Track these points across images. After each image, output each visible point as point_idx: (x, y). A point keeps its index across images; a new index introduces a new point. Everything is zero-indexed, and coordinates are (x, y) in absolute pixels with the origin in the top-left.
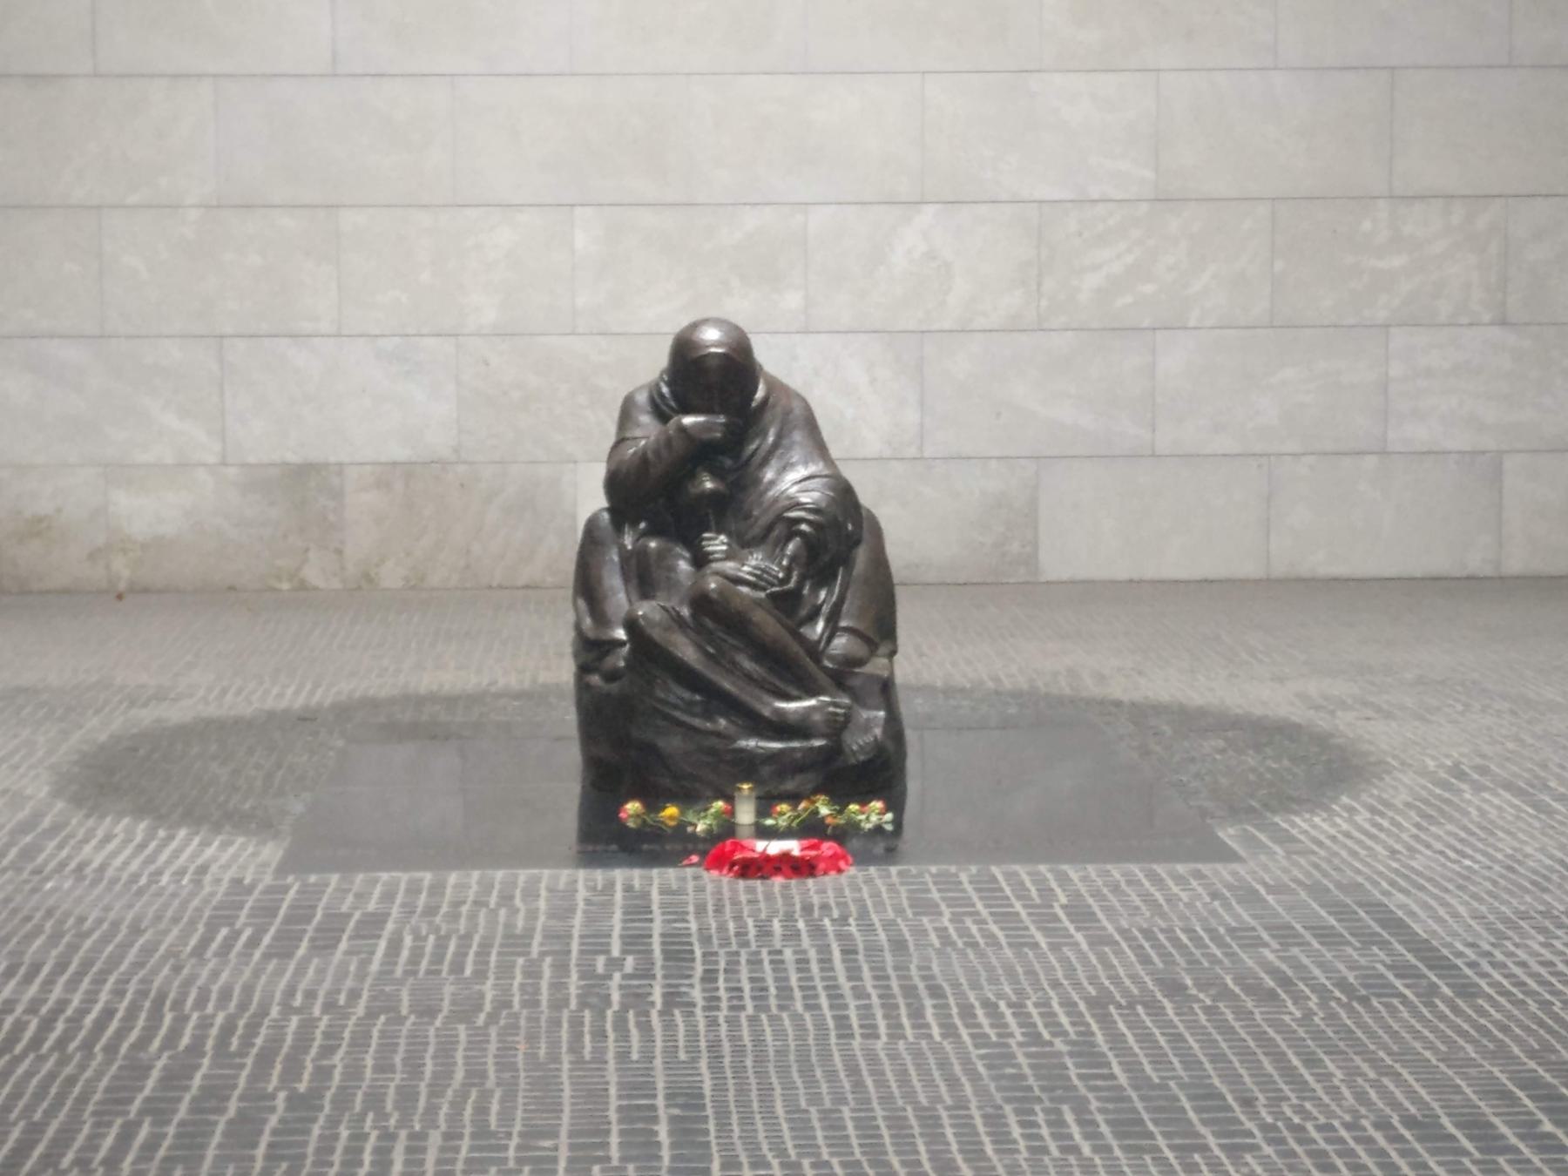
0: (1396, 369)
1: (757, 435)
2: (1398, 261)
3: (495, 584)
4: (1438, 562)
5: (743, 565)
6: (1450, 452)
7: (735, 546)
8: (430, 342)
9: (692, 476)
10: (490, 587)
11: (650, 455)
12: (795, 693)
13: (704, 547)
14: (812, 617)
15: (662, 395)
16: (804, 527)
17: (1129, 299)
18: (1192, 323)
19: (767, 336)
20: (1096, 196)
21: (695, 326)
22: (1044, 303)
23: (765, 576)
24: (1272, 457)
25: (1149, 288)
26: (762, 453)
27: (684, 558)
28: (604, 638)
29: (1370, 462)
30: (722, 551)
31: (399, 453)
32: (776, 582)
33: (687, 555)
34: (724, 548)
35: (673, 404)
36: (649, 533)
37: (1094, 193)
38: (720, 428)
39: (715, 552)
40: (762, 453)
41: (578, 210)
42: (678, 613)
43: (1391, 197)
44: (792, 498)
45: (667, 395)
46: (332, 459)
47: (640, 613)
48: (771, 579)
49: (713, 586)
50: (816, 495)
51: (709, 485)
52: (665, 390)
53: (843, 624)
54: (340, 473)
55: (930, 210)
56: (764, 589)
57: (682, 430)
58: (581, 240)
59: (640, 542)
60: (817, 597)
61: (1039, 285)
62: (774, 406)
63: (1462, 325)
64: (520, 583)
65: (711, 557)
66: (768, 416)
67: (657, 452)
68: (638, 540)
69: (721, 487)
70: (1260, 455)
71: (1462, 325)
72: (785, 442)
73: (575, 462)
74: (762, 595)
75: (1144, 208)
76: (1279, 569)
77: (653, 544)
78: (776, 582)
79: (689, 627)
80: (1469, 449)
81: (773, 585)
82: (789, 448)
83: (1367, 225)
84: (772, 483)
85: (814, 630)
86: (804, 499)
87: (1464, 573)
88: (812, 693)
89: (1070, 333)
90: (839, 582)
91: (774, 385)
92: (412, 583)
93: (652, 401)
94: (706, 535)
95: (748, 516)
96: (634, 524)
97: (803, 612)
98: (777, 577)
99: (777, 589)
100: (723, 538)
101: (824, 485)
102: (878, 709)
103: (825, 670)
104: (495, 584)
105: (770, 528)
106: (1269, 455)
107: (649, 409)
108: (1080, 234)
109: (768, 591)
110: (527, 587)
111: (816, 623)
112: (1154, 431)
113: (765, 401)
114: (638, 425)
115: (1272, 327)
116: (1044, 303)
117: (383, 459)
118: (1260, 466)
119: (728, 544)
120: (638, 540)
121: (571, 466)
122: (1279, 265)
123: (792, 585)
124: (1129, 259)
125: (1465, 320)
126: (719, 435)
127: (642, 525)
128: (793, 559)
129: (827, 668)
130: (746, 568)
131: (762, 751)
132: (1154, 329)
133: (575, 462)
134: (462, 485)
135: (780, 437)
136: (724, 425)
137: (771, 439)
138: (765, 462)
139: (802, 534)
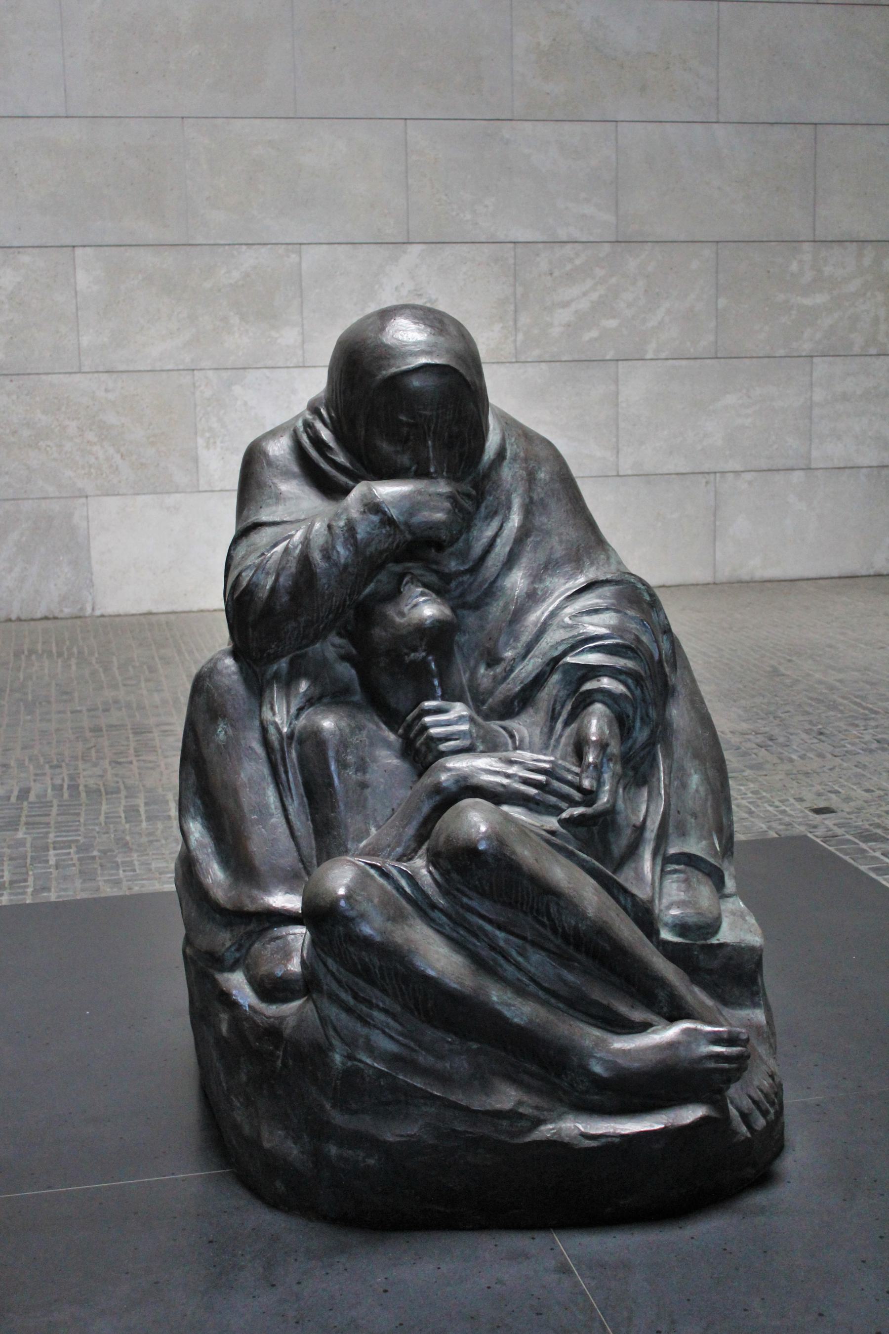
0: (819, 395)
1: (492, 514)
2: (820, 299)
3: (14, 617)
4: (851, 564)
5: (511, 762)
6: (862, 467)
7: (479, 720)
9: (394, 594)
10: (10, 620)
11: (317, 556)
12: (638, 1015)
13: (425, 728)
14: (633, 850)
15: (317, 441)
16: (606, 682)
17: (594, 333)
18: (648, 356)
19: (266, 371)
20: (565, 239)
21: (386, 315)
22: (520, 337)
23: (556, 784)
24: (718, 475)
25: (612, 323)
26: (502, 549)
27: (388, 745)
28: (251, 907)
29: (797, 477)
32: (577, 796)
33: (392, 737)
34: (465, 727)
35: (341, 458)
36: (311, 702)
37: (563, 235)
38: (447, 505)
39: (447, 738)
40: (502, 549)
41: (79, 251)
42: (411, 878)
43: (814, 241)
44: (567, 627)
45: (332, 444)
47: (342, 891)
48: (566, 789)
49: (483, 829)
50: (610, 618)
52: (326, 434)
53: (672, 851)
55: (416, 249)
56: (555, 811)
57: (373, 507)
58: (83, 279)
59: (302, 722)
60: (635, 811)
61: (515, 321)
63: (871, 355)
64: (39, 615)
65: (443, 747)
66: (508, 473)
67: (327, 553)
68: (297, 716)
69: (447, 612)
70: (708, 473)
71: (871, 355)
72: (540, 520)
73: (87, 497)
74: (552, 823)
75: (607, 248)
76: (725, 573)
77: (328, 724)
78: (577, 796)
79: (434, 906)
80: (875, 464)
81: (574, 803)
82: (548, 533)
83: (794, 267)
84: (533, 597)
85: (640, 877)
86: (594, 626)
87: (872, 572)
88: (672, 1019)
89: (543, 365)
90: (662, 768)
91: (509, 424)
93: (299, 450)
94: (429, 704)
95: (493, 660)
96: (288, 683)
97: (620, 845)
98: (579, 788)
99: (578, 811)
100: (459, 709)
101: (619, 596)
102: (755, 1005)
103: (665, 948)
104: (14, 617)
105: (538, 681)
106: (715, 473)
107: (295, 469)
108: (551, 274)
109: (564, 815)
110: (46, 618)
111: (641, 858)
112: (618, 452)
113: (501, 455)
114: (278, 497)
115: (717, 358)
116: (520, 337)
118: (707, 483)
119: (472, 720)
120: (300, 710)
121: (83, 500)
122: (722, 302)
123: (604, 799)
124: (594, 296)
125: (873, 351)
126: (440, 516)
127: (304, 686)
128: (603, 746)
129: (666, 943)
130: (513, 770)
132: (617, 360)
133: (87, 497)
135: (528, 511)
136: (451, 497)
137: (515, 520)
138: (510, 562)
139: (607, 696)
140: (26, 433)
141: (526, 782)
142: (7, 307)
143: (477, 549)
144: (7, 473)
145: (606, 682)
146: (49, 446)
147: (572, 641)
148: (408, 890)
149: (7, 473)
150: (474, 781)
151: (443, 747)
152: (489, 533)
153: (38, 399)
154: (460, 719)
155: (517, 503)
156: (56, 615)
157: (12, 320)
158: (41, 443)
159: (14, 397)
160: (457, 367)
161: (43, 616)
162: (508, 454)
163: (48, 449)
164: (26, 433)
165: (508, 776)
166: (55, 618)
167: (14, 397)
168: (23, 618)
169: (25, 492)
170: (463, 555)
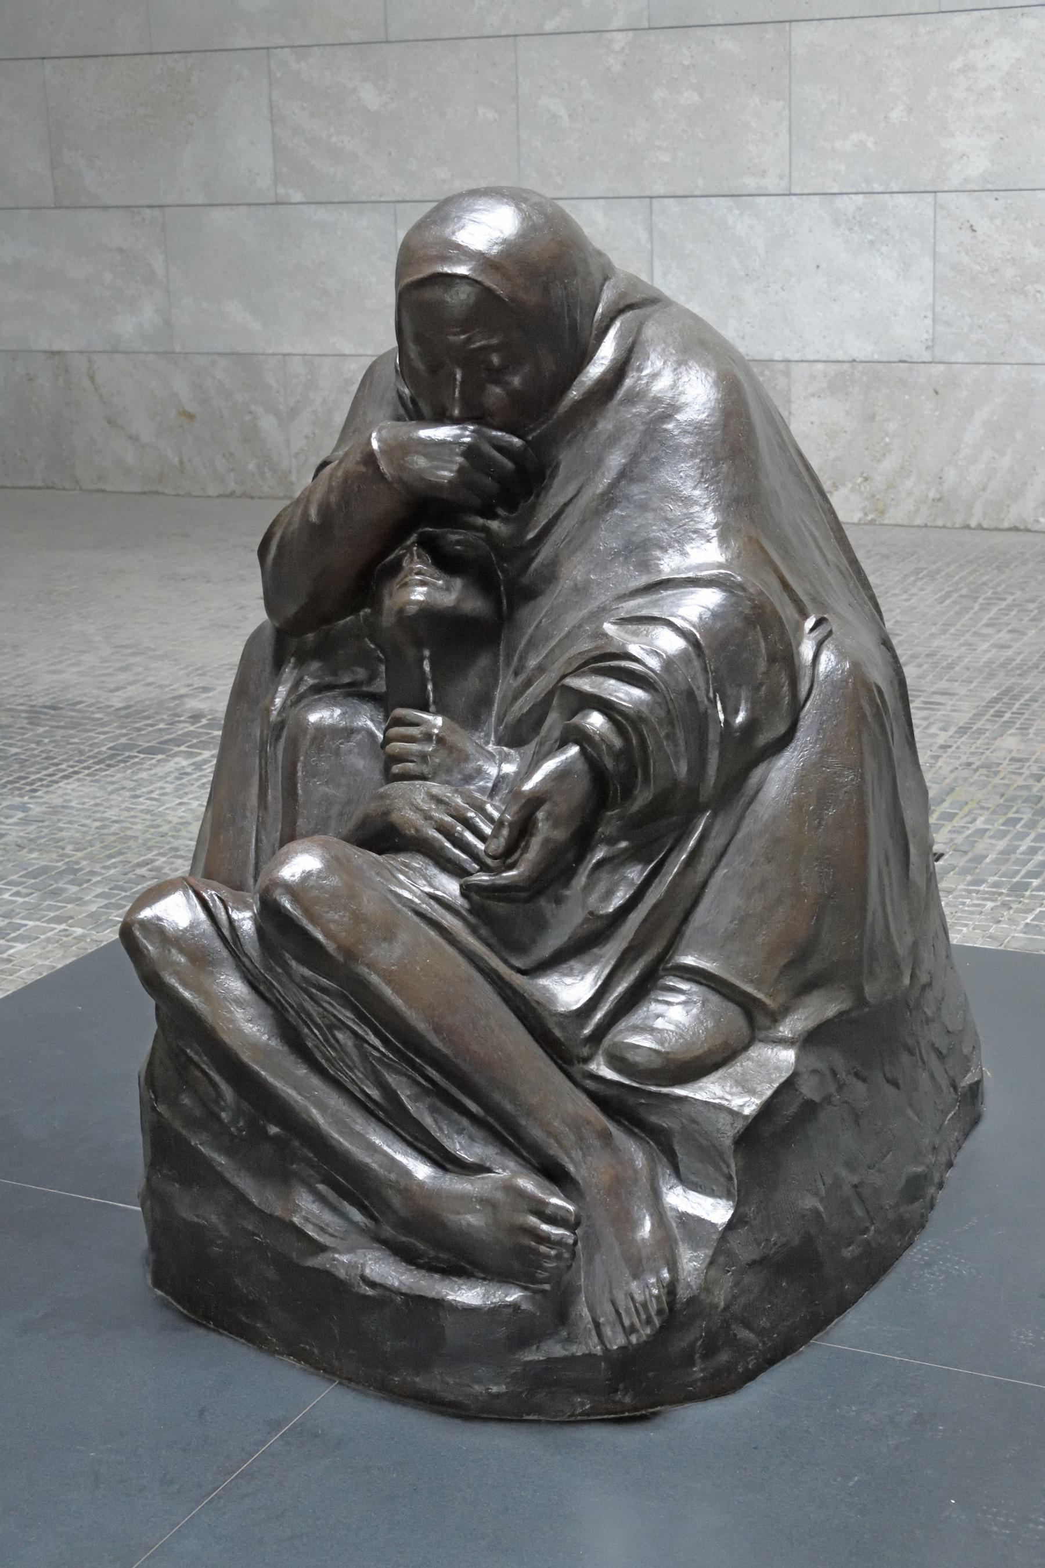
3: (973, 523)
8: (901, 199)
10: (968, 527)
30: (424, 757)
31: (859, 348)
36: (321, 691)
46: (778, 356)
51: (419, 594)
54: (788, 374)
60: (609, 894)
62: (633, 398)
64: (1006, 525)
74: (450, 887)
92: (870, 517)
96: (302, 660)
104: (973, 523)
110: (1015, 529)
117: (840, 355)
128: (536, 801)
131: (370, 1292)
134: (937, 393)
135: (623, 474)
136: (471, 452)
140: (1010, 272)
141: (442, 829)
142: (999, 94)
143: (542, 519)
144: (980, 327)
145: (596, 720)
146: (1039, 292)
147: (586, 657)
148: (226, 933)
149: (980, 327)
150: (395, 817)
151: (396, 769)
152: (562, 500)
153: (1029, 225)
154: (428, 737)
155: (616, 460)
156: (1029, 526)
157: (1005, 113)
158: (1029, 287)
159: (998, 222)
160: (479, 279)
161: (1012, 525)
162: (621, 393)
163: (1038, 295)
164: (1010, 272)
165: (428, 817)
166: (1028, 530)
167: (998, 222)
168: (985, 526)
169: (1003, 354)
170: (524, 524)
